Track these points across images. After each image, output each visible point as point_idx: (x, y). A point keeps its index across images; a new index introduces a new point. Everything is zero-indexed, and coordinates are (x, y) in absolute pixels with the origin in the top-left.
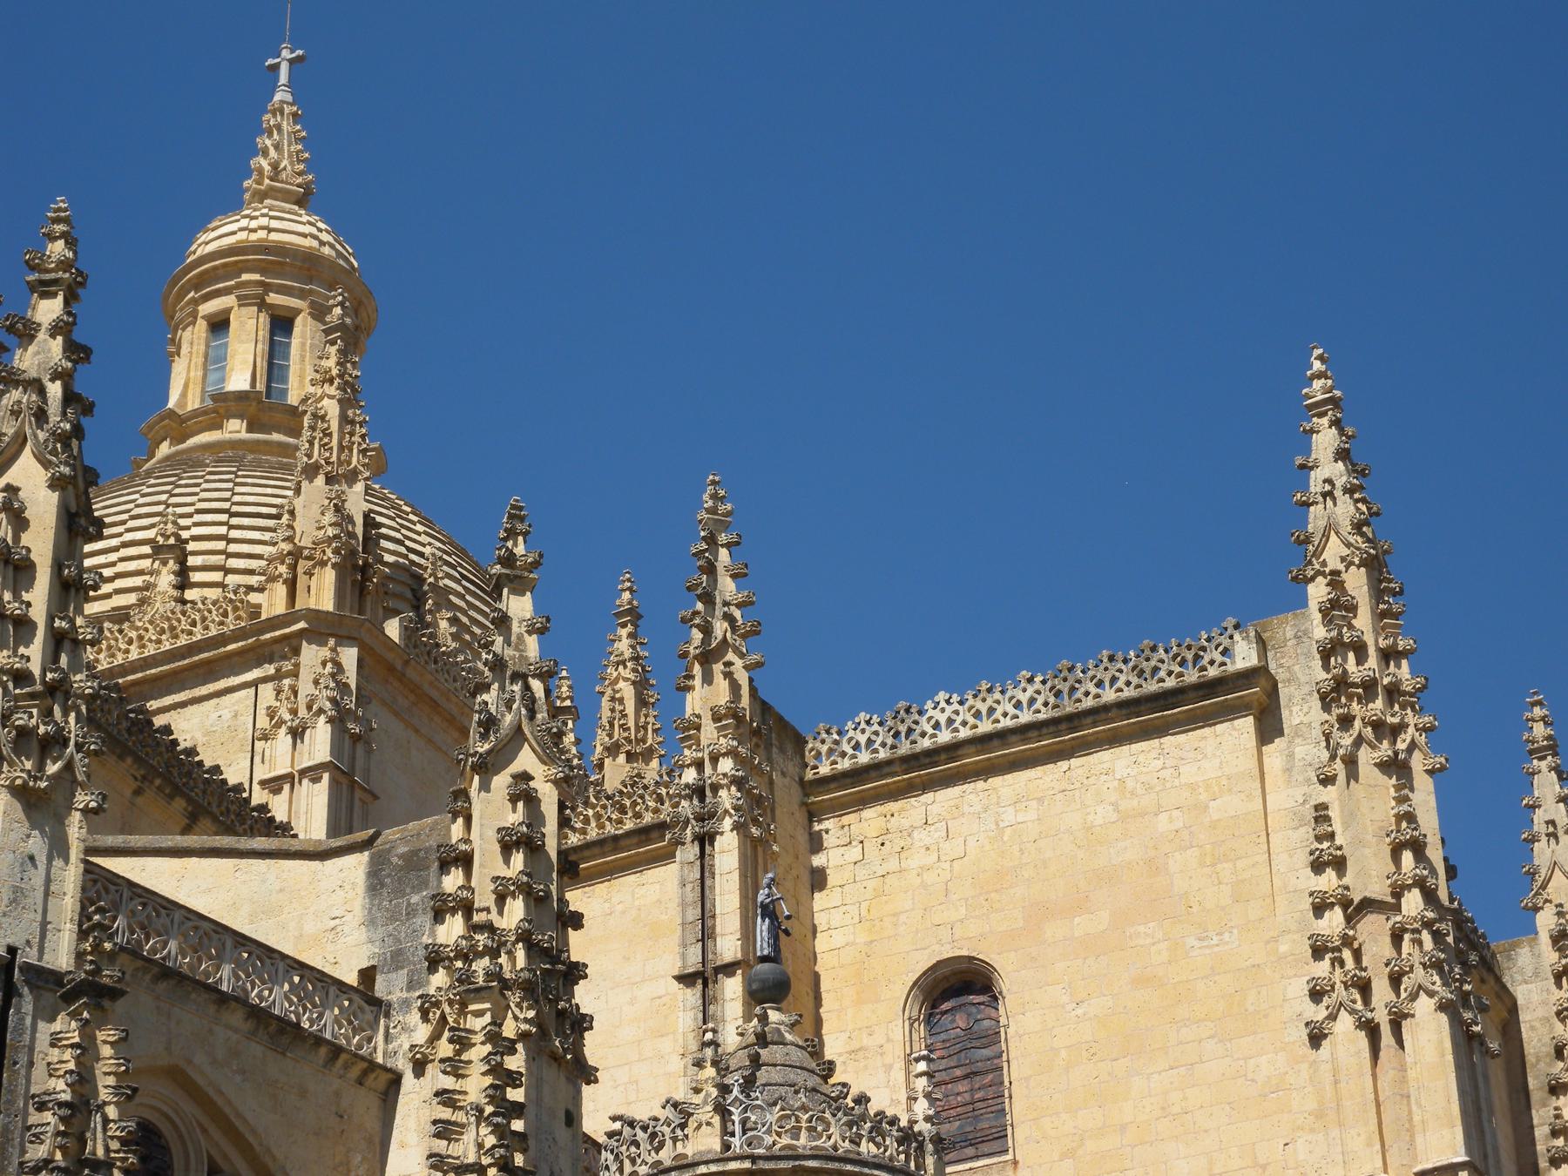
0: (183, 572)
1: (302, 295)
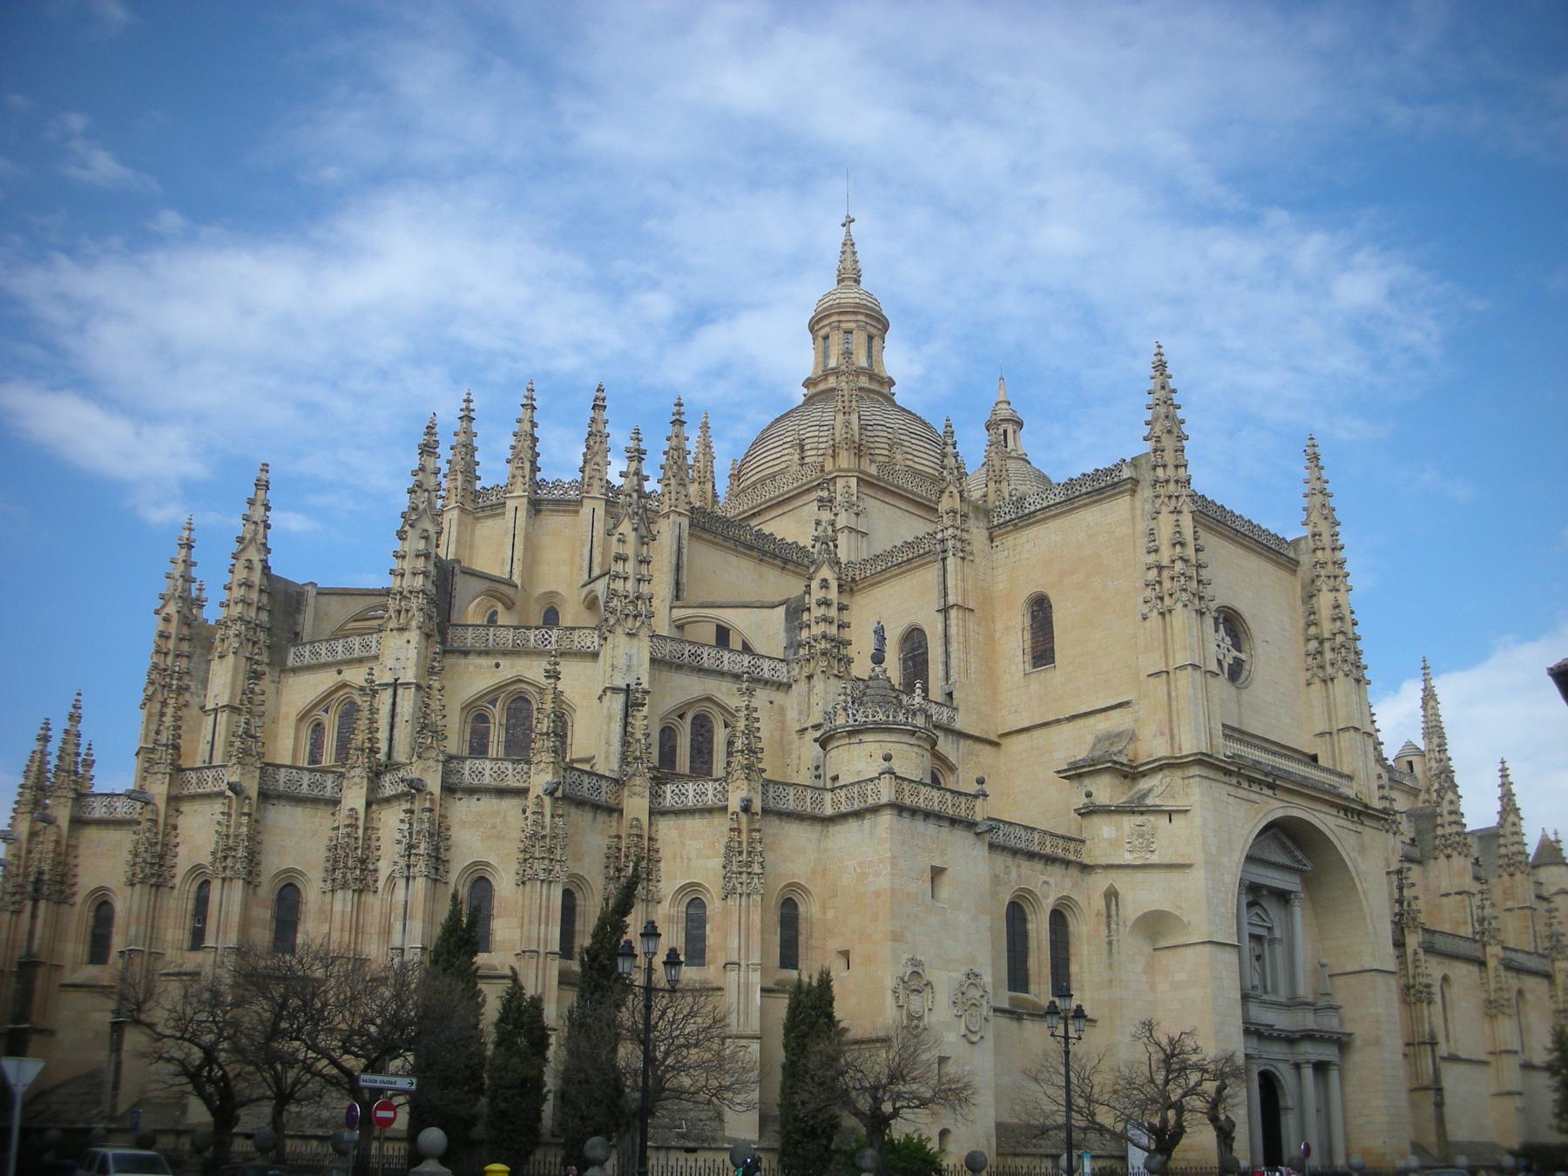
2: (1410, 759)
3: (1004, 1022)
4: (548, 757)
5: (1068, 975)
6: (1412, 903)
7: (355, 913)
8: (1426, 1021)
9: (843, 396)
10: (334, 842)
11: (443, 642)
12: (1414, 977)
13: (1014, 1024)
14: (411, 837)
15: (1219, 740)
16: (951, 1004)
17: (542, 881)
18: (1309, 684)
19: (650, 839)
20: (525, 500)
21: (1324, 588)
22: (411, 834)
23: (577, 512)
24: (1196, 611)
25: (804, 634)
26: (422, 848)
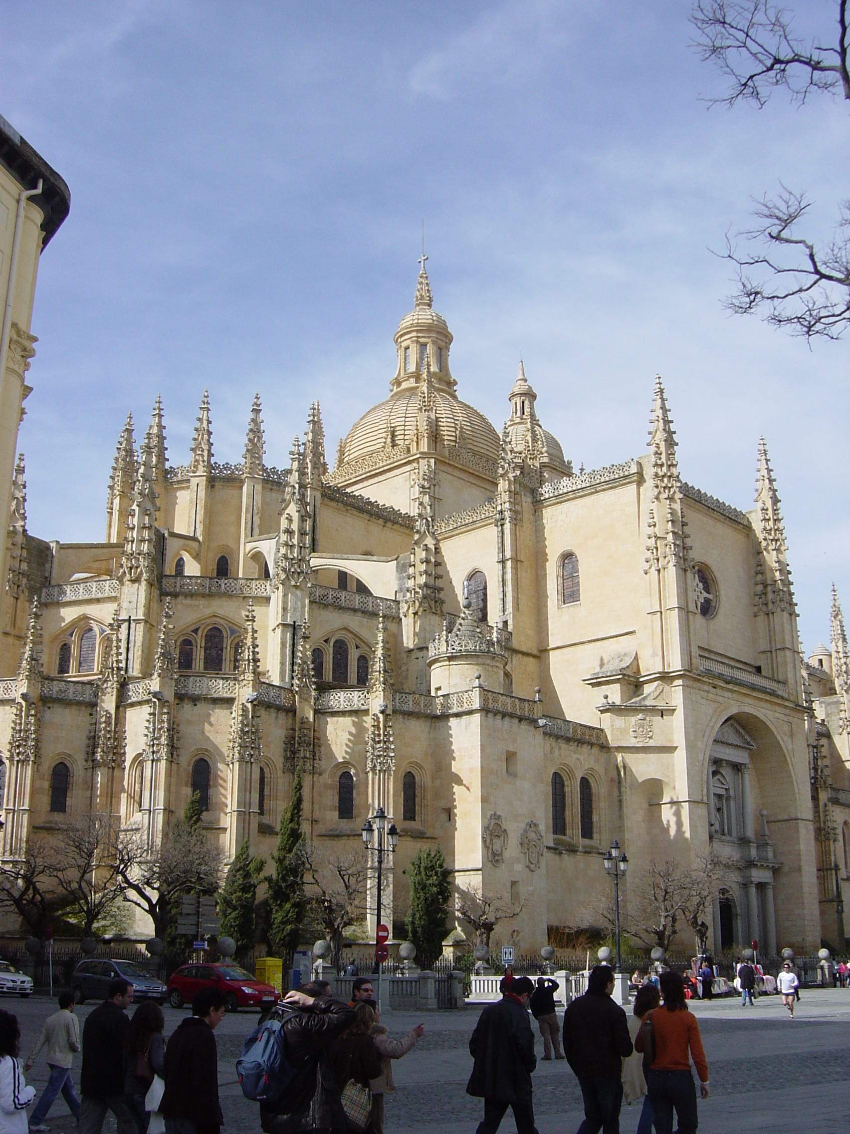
0: (393, 436)
1: (429, 337)
2: (820, 657)
3: (548, 855)
4: (249, 676)
5: (592, 823)
6: (824, 770)
7: (110, 784)
8: (832, 853)
9: (424, 397)
10: (92, 734)
11: (160, 589)
12: (825, 823)
13: (557, 857)
14: (154, 732)
15: (696, 661)
16: (519, 845)
17: (247, 762)
18: (756, 616)
19: (314, 731)
20: (205, 478)
21: (770, 548)
22: (154, 730)
23: (241, 488)
24: (682, 569)
25: (410, 583)
26: (164, 740)
